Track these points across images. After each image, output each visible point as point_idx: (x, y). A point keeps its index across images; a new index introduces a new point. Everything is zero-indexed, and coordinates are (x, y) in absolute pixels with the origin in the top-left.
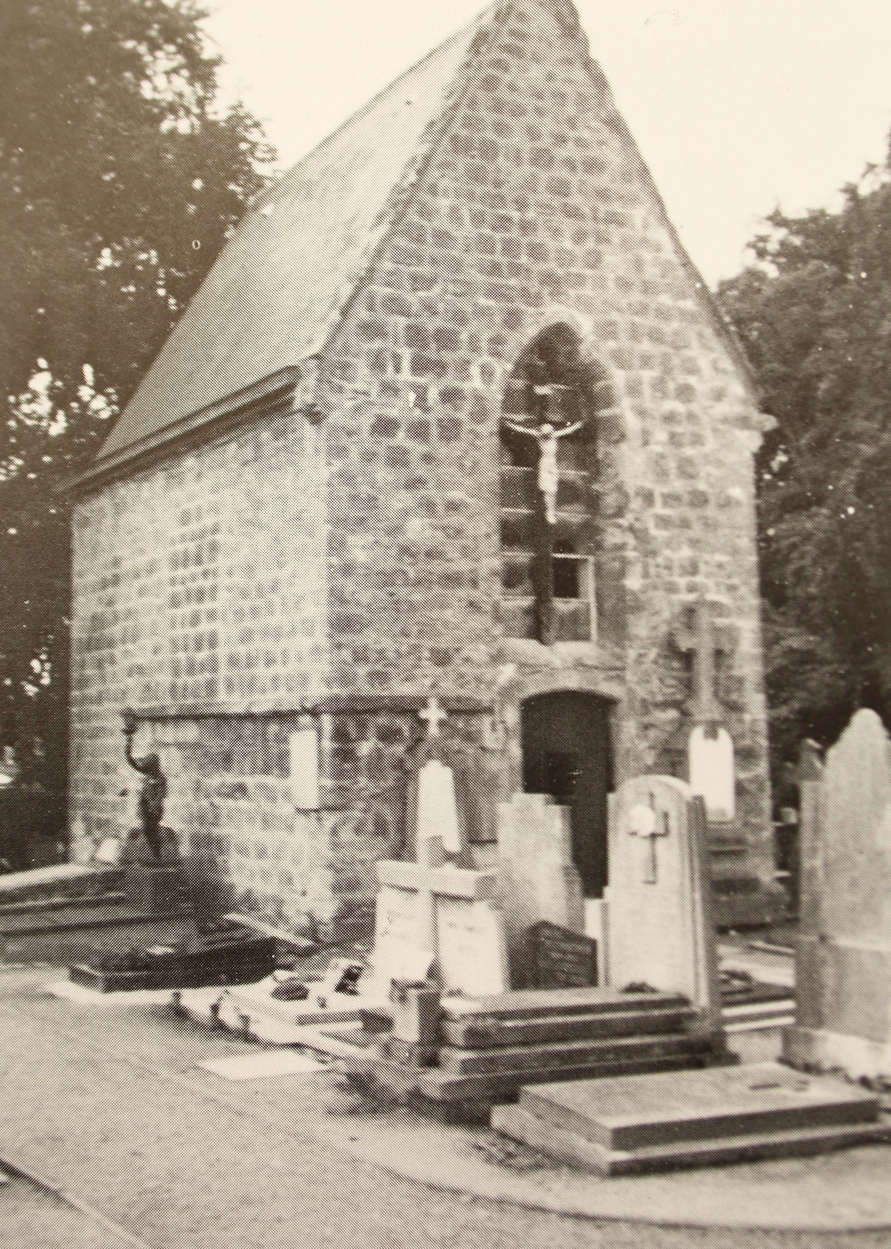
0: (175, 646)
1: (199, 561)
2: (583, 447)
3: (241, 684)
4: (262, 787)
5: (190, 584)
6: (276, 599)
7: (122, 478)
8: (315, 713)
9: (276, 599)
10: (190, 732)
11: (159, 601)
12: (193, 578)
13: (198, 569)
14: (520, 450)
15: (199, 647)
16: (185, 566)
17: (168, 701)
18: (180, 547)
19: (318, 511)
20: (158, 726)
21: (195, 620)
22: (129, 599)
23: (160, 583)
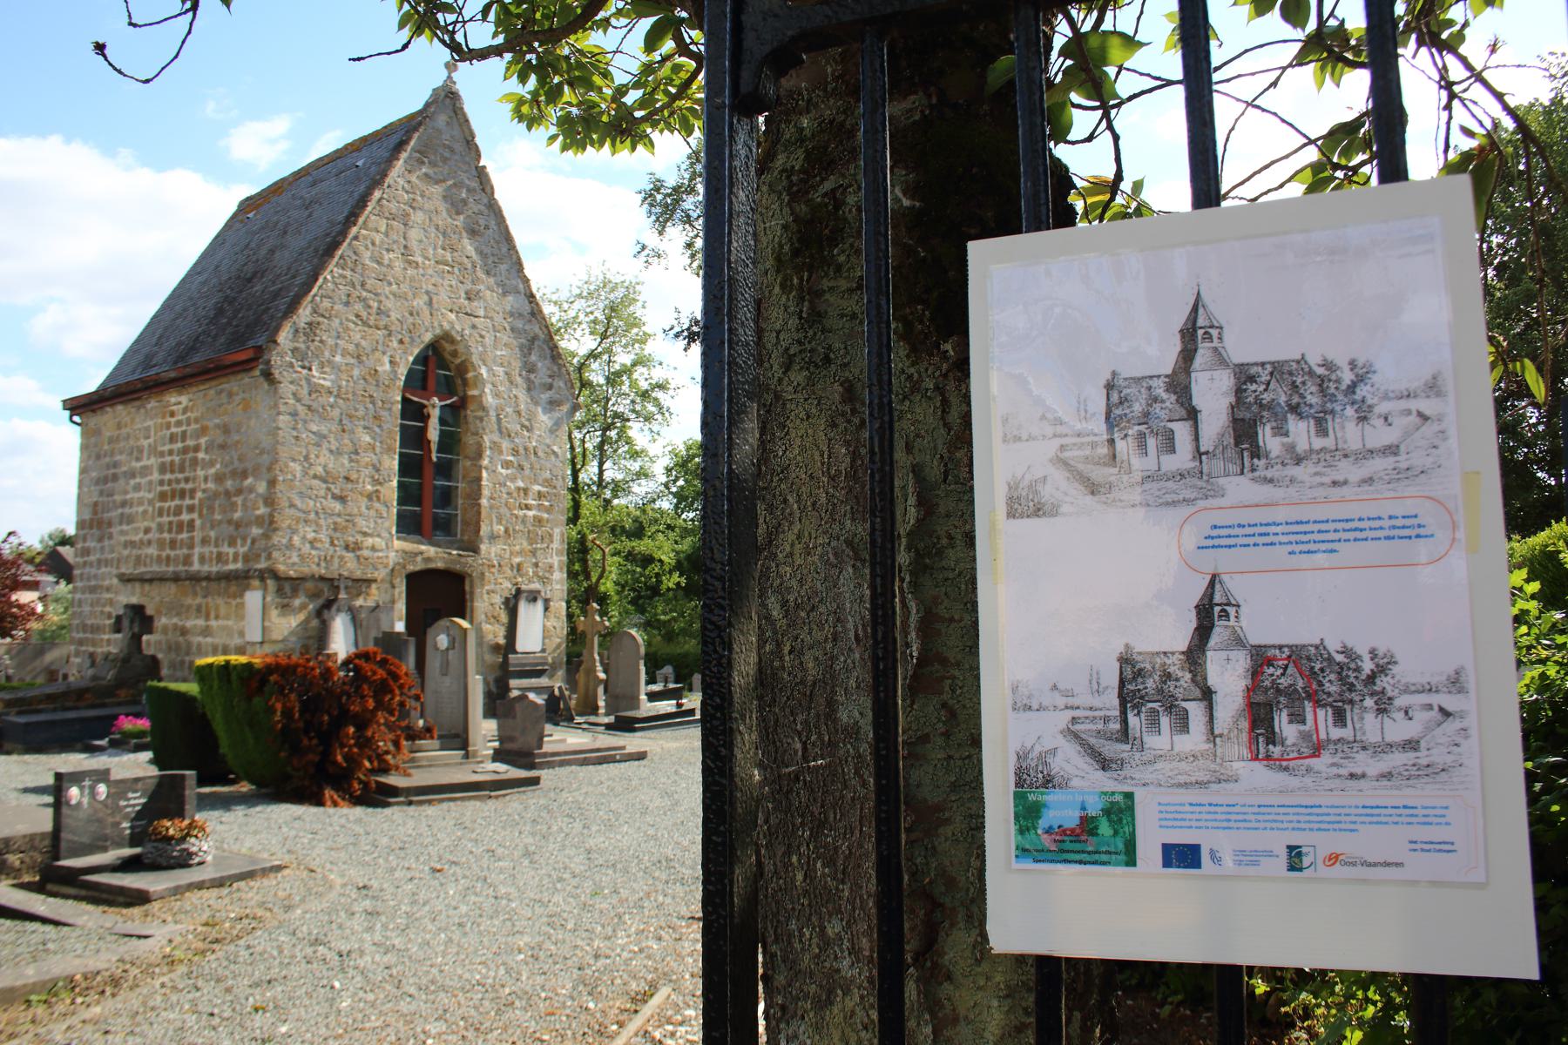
0: (160, 528)
1: (182, 470)
2: (456, 413)
4: (224, 628)
5: (174, 486)
8: (262, 579)
9: (239, 500)
10: (171, 589)
11: (150, 496)
12: (178, 481)
13: (180, 476)
14: (413, 411)
16: (172, 472)
17: (155, 568)
18: (168, 459)
20: (147, 587)
22: (126, 492)
23: (150, 482)
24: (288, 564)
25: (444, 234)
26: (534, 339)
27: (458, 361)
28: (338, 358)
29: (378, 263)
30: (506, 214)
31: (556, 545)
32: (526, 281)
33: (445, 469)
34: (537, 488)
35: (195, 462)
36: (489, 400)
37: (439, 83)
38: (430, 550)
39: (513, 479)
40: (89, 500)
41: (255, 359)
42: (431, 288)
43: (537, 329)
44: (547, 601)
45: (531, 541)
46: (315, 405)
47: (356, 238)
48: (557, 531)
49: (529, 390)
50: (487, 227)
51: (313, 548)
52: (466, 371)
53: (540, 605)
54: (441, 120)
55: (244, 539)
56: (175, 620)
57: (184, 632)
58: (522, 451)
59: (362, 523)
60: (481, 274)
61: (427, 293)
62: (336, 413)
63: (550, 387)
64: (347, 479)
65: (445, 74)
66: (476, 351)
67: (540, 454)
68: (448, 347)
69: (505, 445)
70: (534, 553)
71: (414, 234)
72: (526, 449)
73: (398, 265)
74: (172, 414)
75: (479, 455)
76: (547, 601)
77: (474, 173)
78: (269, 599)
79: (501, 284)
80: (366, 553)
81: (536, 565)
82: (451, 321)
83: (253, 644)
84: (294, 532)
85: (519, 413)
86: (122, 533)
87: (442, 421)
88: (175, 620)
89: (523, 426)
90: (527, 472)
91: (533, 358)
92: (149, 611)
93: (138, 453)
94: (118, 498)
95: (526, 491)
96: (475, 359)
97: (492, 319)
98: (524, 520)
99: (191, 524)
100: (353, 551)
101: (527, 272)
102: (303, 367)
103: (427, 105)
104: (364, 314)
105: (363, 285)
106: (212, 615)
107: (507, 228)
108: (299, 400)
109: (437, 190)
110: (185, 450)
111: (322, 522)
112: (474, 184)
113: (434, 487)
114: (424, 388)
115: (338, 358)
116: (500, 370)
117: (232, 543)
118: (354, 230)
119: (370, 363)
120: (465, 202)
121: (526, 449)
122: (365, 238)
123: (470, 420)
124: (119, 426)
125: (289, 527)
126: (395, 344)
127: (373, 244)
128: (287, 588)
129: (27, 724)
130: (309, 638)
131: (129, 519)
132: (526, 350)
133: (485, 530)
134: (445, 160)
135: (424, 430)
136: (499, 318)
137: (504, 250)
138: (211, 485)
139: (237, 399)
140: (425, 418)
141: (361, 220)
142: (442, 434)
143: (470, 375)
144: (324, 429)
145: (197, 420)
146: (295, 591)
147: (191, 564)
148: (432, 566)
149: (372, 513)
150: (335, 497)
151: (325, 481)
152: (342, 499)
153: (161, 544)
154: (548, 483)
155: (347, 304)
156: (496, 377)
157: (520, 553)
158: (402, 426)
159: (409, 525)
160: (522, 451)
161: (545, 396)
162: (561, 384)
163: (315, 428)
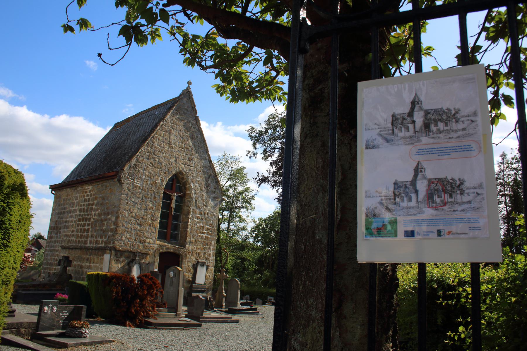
0: (77, 231)
1: (87, 211)
4: (96, 266)
6: (105, 223)
7: (70, 188)
8: (111, 250)
9: (105, 223)
11: (75, 220)
12: (85, 215)
13: (86, 213)
14: (167, 197)
15: (84, 232)
16: (84, 212)
17: (74, 244)
18: (83, 207)
20: (70, 251)
21: (84, 225)
22: (67, 218)
23: (76, 215)
24: (119, 246)
25: (183, 138)
26: (210, 175)
28: (143, 177)
29: (160, 146)
30: (204, 133)
31: (212, 247)
33: (176, 218)
34: (207, 226)
35: (92, 209)
36: (193, 195)
38: (169, 245)
39: (199, 223)
40: (54, 220)
41: (116, 175)
42: (177, 155)
43: (211, 172)
44: (207, 267)
45: (204, 245)
46: (134, 192)
47: (153, 137)
48: (213, 242)
49: (207, 193)
50: (197, 137)
51: (129, 241)
53: (205, 267)
54: (185, 100)
55: (106, 236)
56: (79, 263)
57: (81, 267)
58: (203, 213)
59: (146, 234)
60: (193, 152)
61: (175, 157)
62: (141, 195)
63: (214, 192)
64: (143, 218)
66: (190, 177)
67: (209, 215)
69: (197, 211)
70: (204, 249)
71: (173, 137)
72: (204, 213)
73: (166, 147)
74: (86, 192)
75: (189, 214)
76: (207, 267)
78: (112, 257)
79: (200, 156)
80: (147, 244)
81: (205, 253)
82: (182, 167)
84: (123, 235)
85: (203, 200)
86: (64, 232)
87: (177, 201)
88: (79, 263)
89: (204, 205)
90: (204, 221)
91: (209, 182)
92: (71, 259)
93: (73, 205)
94: (64, 220)
95: (203, 227)
96: (189, 181)
97: (196, 168)
98: (202, 237)
99: (88, 230)
100: (143, 243)
101: (209, 153)
102: (132, 179)
103: (180, 95)
104: (154, 163)
105: (154, 153)
106: (92, 262)
107: (204, 137)
108: (129, 190)
109: (181, 123)
110: (89, 205)
111: (133, 232)
112: (194, 122)
113: (172, 224)
114: (172, 189)
115: (143, 177)
116: (198, 185)
117: (101, 237)
118: (153, 134)
119: (154, 179)
121: (204, 213)
122: (156, 137)
124: (67, 195)
125: (122, 233)
126: (163, 174)
127: (159, 140)
128: (119, 254)
131: (67, 227)
132: (207, 179)
133: (188, 239)
134: (185, 114)
135: (170, 203)
136: (199, 168)
137: (202, 145)
138: (96, 217)
139: (108, 188)
140: (171, 200)
141: (155, 132)
142: (176, 206)
143: (188, 186)
144: (136, 201)
145: (94, 195)
146: (121, 256)
147: (87, 244)
148: (169, 251)
149: (150, 231)
150: (138, 224)
151: (135, 219)
152: (140, 225)
153: (77, 236)
154: (211, 225)
155: (148, 159)
156: (196, 187)
157: (199, 249)
159: (162, 236)
160: (203, 213)
161: (212, 195)
163: (133, 200)
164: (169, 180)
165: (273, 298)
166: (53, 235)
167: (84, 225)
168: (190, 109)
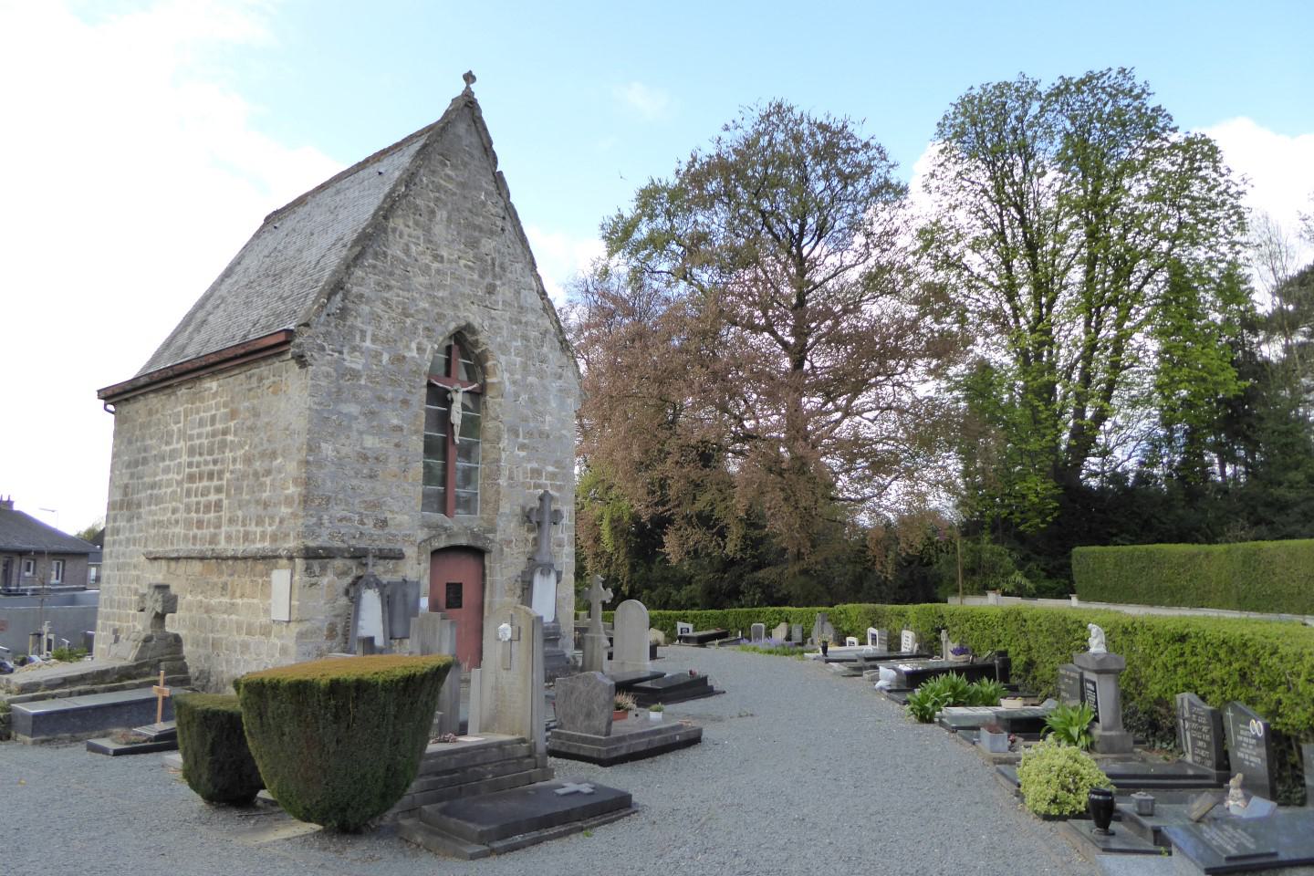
0: (188, 509)
1: (211, 452)
2: (477, 396)
3: (238, 539)
4: (249, 606)
5: (203, 468)
8: (291, 558)
9: (268, 480)
10: (197, 566)
11: (179, 478)
12: (206, 463)
14: (439, 396)
17: (182, 546)
18: (197, 442)
19: (300, 424)
20: (173, 564)
21: (205, 492)
26: (545, 333)
27: (480, 350)
31: (565, 521)
32: (538, 278)
33: (467, 452)
35: (223, 445)
37: (459, 93)
41: (286, 342)
44: (559, 574)
52: (487, 360)
54: (461, 128)
55: (272, 518)
56: (200, 597)
63: (560, 377)
65: (464, 85)
68: (470, 338)
73: (427, 259)
75: (499, 438)
76: (559, 574)
77: (491, 177)
78: (297, 578)
82: (474, 316)
83: (280, 622)
86: (150, 512)
87: (464, 407)
88: (200, 597)
91: (545, 349)
99: (218, 505)
101: (540, 270)
106: (238, 594)
112: (492, 188)
114: (448, 374)
117: (259, 522)
120: (484, 204)
123: (489, 405)
124: (150, 413)
129: (36, 716)
130: (337, 616)
131: (157, 500)
134: (465, 165)
135: (447, 414)
137: (519, 251)
138: (239, 466)
140: (448, 403)
142: (464, 418)
143: (489, 364)
147: (217, 544)
153: (188, 524)
158: (428, 411)
162: (570, 374)
164: (438, 352)
165: (690, 626)
166: (121, 524)
167: (205, 492)
168: (477, 153)
